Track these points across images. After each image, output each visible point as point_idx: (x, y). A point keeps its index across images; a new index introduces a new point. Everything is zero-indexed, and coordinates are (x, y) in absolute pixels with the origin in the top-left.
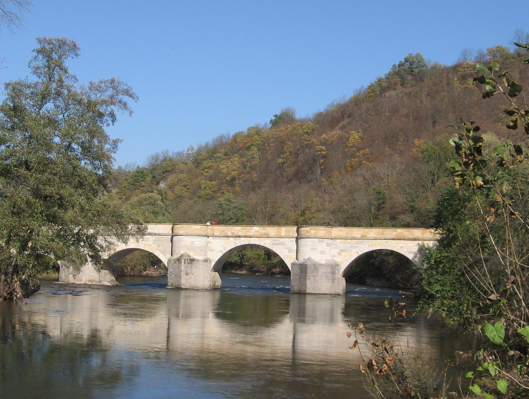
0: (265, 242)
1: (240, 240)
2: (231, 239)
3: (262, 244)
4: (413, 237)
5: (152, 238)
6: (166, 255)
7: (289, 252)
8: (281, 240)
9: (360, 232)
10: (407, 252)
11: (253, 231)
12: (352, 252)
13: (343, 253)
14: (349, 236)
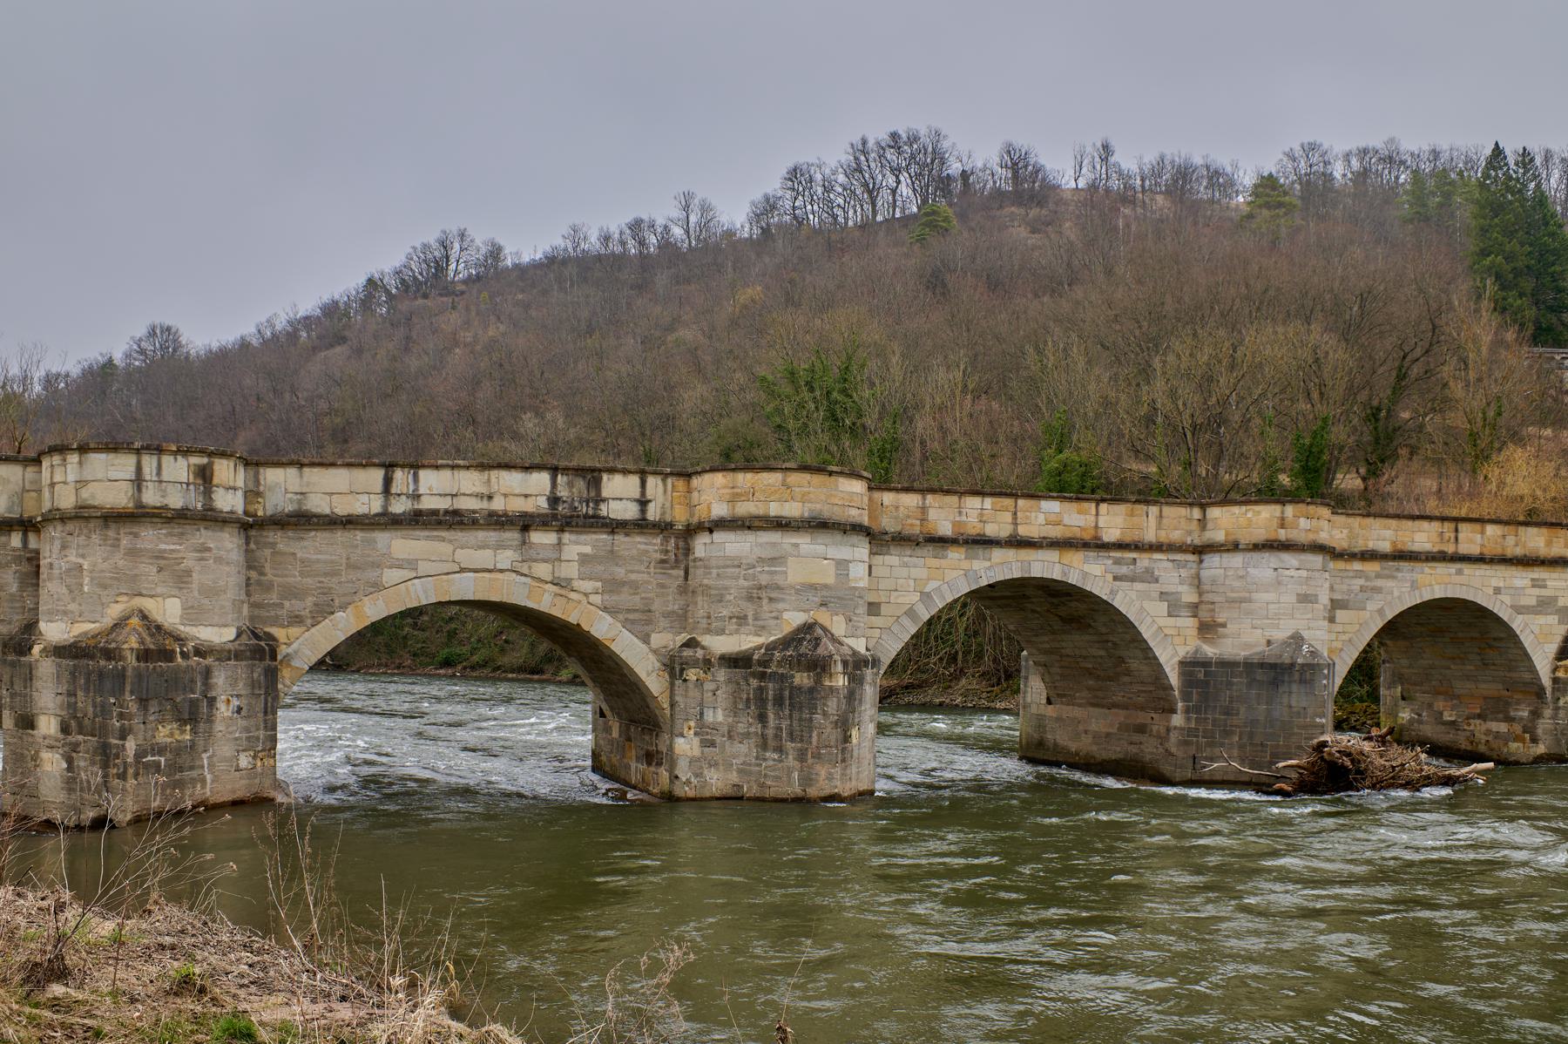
0: (1087, 568)
1: (990, 560)
2: (955, 555)
3: (1074, 579)
4: (1519, 551)
5: (577, 543)
6: (653, 635)
7: (1169, 616)
8: (1144, 560)
9: (1388, 533)
10: (1511, 607)
11: (1041, 518)
12: (1364, 609)
13: (1340, 615)
14: (1360, 546)
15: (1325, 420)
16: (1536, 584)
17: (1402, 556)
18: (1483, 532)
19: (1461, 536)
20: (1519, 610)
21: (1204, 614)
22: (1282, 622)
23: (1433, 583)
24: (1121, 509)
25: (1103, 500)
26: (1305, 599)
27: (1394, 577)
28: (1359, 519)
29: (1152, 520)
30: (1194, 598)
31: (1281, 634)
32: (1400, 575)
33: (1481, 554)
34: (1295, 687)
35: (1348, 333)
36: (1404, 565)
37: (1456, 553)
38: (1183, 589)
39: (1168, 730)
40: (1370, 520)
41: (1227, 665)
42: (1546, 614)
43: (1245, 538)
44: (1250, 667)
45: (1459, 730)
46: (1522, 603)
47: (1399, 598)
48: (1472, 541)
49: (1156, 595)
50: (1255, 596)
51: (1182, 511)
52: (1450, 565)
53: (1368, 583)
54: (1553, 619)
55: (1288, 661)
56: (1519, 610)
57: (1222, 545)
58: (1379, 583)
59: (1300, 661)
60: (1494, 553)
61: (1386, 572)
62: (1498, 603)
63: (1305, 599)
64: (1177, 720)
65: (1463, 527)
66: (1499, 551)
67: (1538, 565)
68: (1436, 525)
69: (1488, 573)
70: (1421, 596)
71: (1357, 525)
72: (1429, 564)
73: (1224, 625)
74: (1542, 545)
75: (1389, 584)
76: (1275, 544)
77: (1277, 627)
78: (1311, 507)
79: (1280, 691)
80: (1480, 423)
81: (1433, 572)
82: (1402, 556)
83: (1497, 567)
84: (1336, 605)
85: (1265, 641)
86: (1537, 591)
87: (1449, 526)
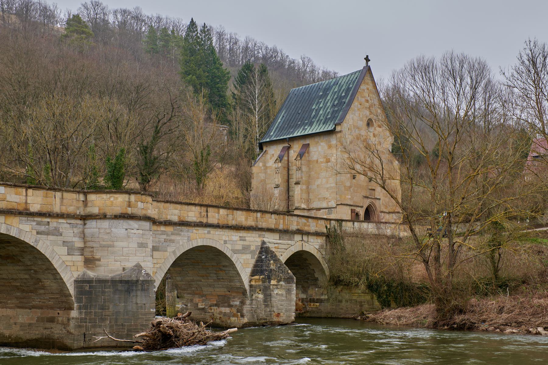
4: (234, 223)
9: (176, 212)
10: (232, 250)
14: (163, 218)
15: (122, 151)
16: (242, 239)
17: (183, 224)
18: (218, 213)
19: (209, 214)
20: (235, 251)
21: (88, 254)
22: (130, 258)
23: (198, 238)
24: (41, 193)
25: (30, 188)
26: (142, 245)
27: (180, 235)
28: (163, 204)
29: (58, 200)
30: (81, 245)
31: (130, 265)
32: (183, 233)
33: (218, 223)
34: (139, 293)
35: (131, 106)
36: (184, 228)
37: (207, 223)
38: (76, 239)
39: (69, 320)
40: (168, 205)
41: (102, 282)
42: (246, 254)
43: (110, 212)
44: (114, 282)
45: (205, 312)
46: (236, 249)
47: (182, 245)
48: (213, 217)
49: (61, 243)
50: (116, 244)
51: (74, 196)
52: (205, 229)
53: (168, 238)
54: (249, 256)
55: (135, 279)
56: (235, 251)
57: (97, 216)
58: (173, 237)
59: (141, 279)
60: (224, 223)
61: (176, 232)
62: (226, 248)
63: (142, 245)
64: (74, 314)
65: (210, 209)
66: (225, 222)
67: (243, 230)
68: (198, 208)
69: (221, 233)
70: (192, 245)
71: (162, 207)
72: (196, 228)
73: (99, 260)
74: (243, 220)
75: (177, 238)
76: (126, 216)
77: (128, 260)
78: (144, 197)
79: (131, 295)
80: (200, 158)
81: (197, 232)
82: (183, 224)
83: (224, 230)
84: (155, 249)
85: (121, 269)
86: (242, 243)
87: (204, 209)
